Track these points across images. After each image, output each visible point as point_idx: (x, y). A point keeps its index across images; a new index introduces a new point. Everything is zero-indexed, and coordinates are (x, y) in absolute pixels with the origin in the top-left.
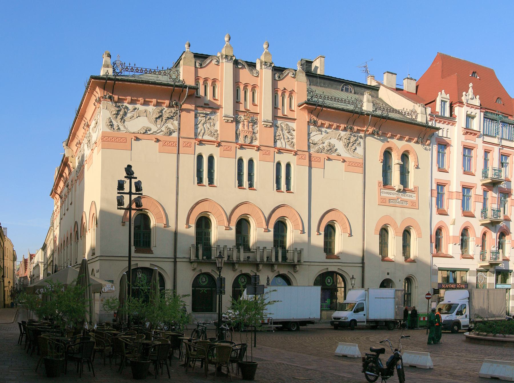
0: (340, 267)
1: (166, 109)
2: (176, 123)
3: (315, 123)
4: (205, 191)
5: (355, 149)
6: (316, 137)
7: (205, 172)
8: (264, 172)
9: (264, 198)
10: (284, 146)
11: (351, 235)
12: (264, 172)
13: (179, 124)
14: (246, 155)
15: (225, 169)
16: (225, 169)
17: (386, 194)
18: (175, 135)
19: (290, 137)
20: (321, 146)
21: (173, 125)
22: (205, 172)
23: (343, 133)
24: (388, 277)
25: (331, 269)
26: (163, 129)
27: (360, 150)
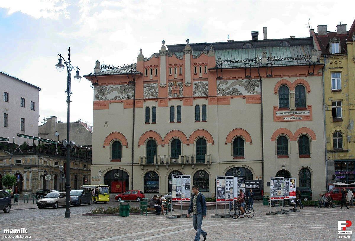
0: (245, 164)
1: (127, 85)
2: (133, 92)
3: (221, 78)
4: (151, 126)
5: (255, 89)
6: (223, 86)
7: (151, 117)
8: (188, 112)
9: (188, 126)
10: (200, 95)
11: (251, 143)
12: (188, 112)
13: (134, 92)
14: (175, 103)
15: (163, 113)
16: (163, 113)
17: (280, 114)
18: (132, 98)
19: (204, 89)
20: (227, 91)
21: (130, 94)
22: (151, 117)
23: (244, 81)
24: (283, 168)
25: (237, 166)
26: (126, 96)
27: (258, 89)
